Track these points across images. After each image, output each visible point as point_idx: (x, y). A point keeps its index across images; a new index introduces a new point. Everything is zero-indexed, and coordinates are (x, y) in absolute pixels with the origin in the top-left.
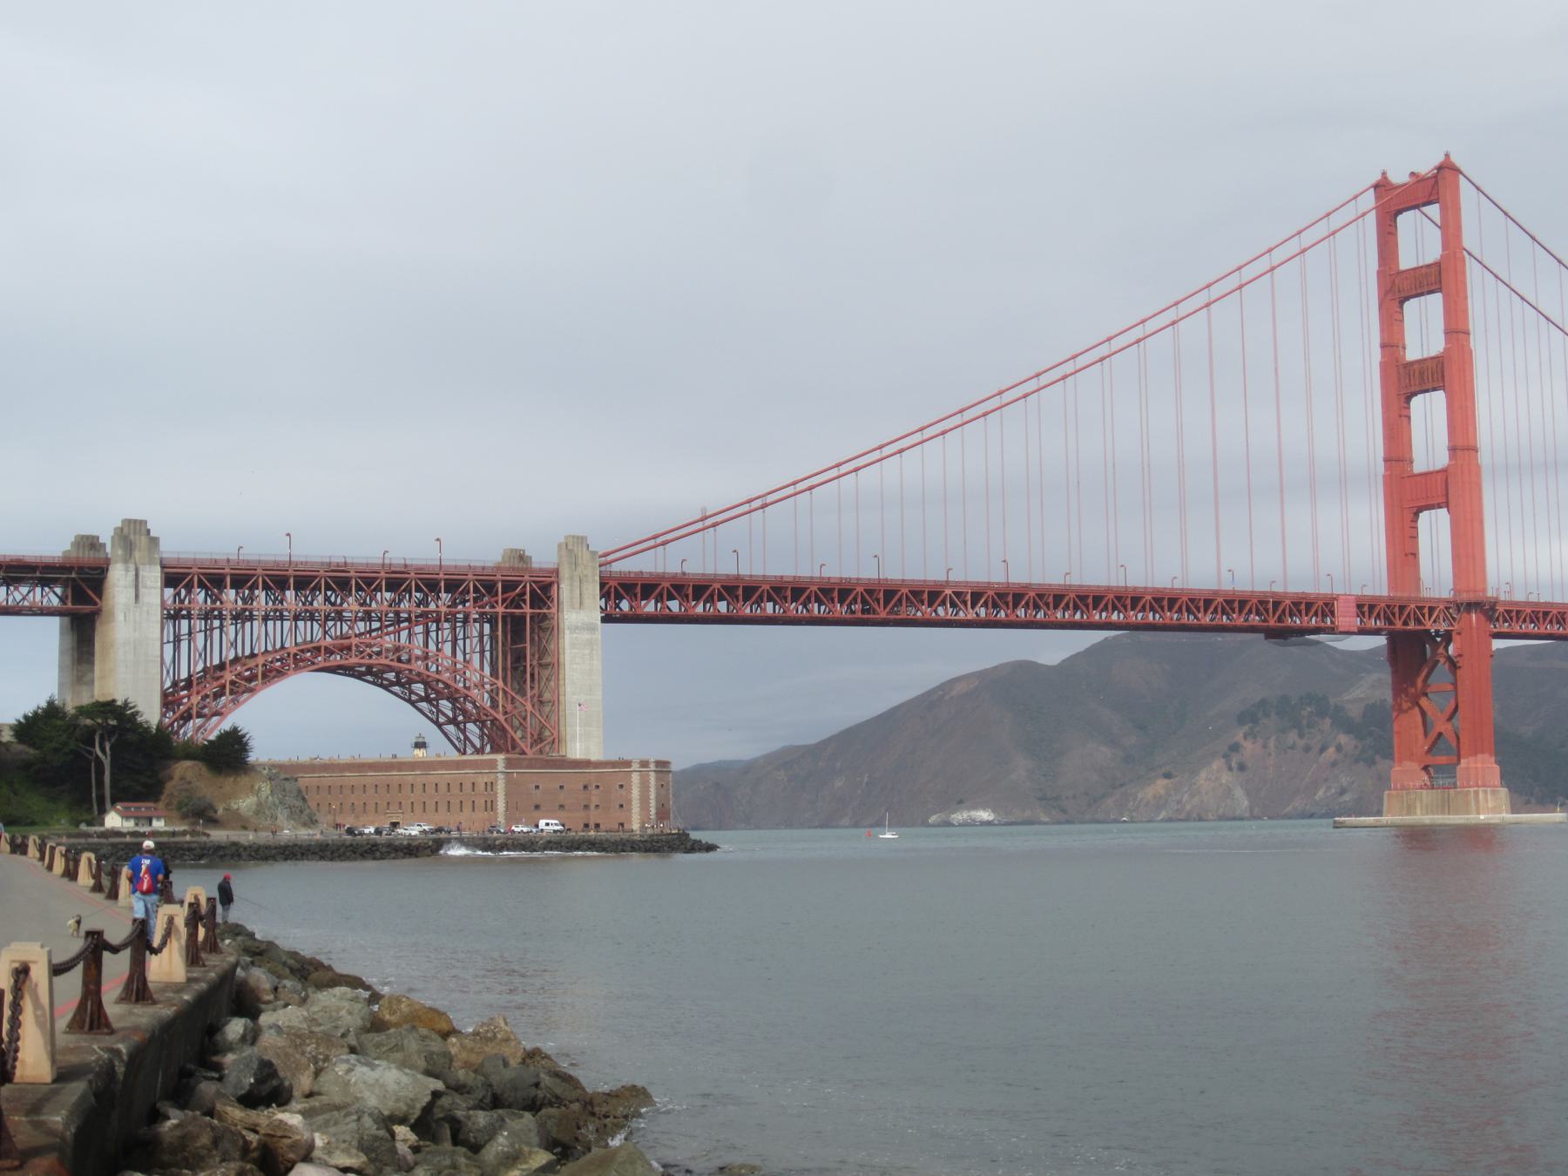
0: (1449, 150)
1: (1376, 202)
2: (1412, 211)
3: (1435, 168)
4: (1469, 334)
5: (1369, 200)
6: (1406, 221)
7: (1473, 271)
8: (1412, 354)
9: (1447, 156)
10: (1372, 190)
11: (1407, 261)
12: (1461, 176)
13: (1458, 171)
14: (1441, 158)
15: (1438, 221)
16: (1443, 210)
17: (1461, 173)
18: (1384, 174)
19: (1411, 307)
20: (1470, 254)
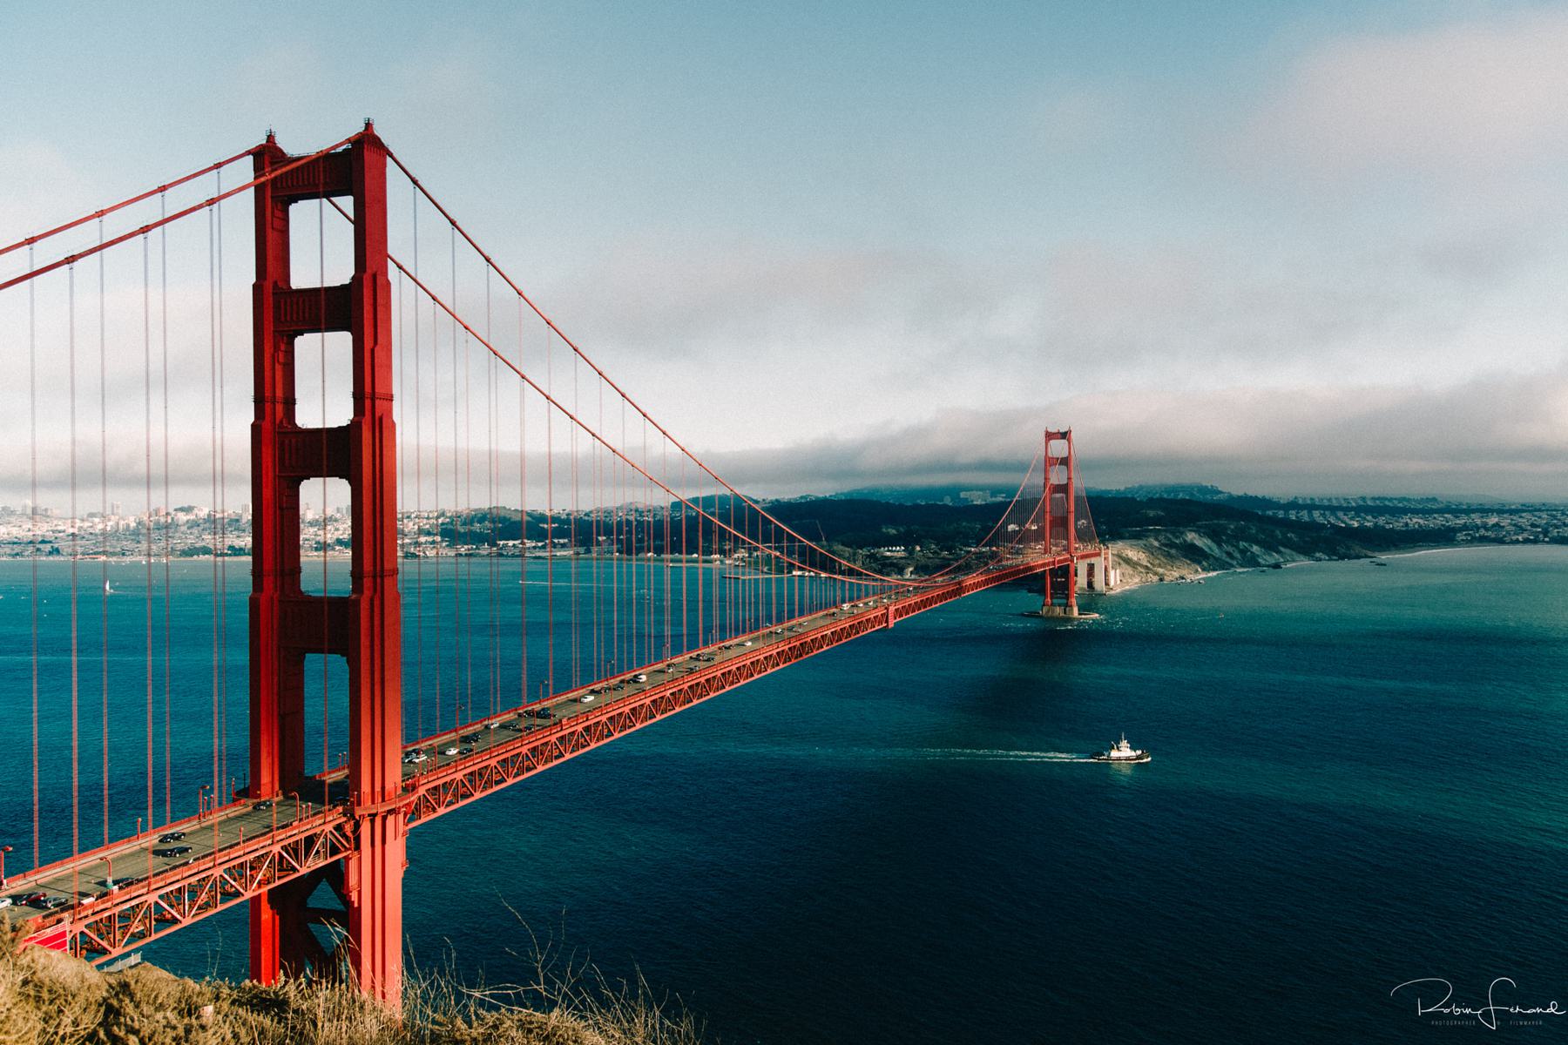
0: (372, 118)
1: (255, 178)
2: (316, 202)
3: (349, 140)
4: (392, 400)
5: (244, 171)
6: (304, 216)
7: (404, 302)
8: (308, 416)
9: (368, 125)
10: (251, 157)
11: (302, 277)
12: (389, 160)
13: (383, 151)
14: (361, 128)
15: (352, 216)
16: (359, 207)
17: (391, 156)
18: (270, 138)
19: (307, 346)
20: (400, 267)
